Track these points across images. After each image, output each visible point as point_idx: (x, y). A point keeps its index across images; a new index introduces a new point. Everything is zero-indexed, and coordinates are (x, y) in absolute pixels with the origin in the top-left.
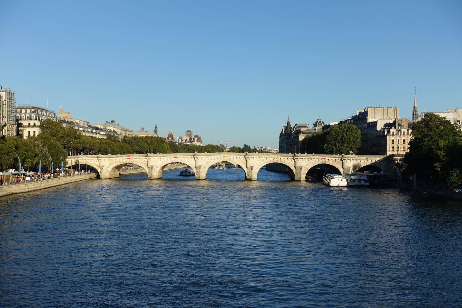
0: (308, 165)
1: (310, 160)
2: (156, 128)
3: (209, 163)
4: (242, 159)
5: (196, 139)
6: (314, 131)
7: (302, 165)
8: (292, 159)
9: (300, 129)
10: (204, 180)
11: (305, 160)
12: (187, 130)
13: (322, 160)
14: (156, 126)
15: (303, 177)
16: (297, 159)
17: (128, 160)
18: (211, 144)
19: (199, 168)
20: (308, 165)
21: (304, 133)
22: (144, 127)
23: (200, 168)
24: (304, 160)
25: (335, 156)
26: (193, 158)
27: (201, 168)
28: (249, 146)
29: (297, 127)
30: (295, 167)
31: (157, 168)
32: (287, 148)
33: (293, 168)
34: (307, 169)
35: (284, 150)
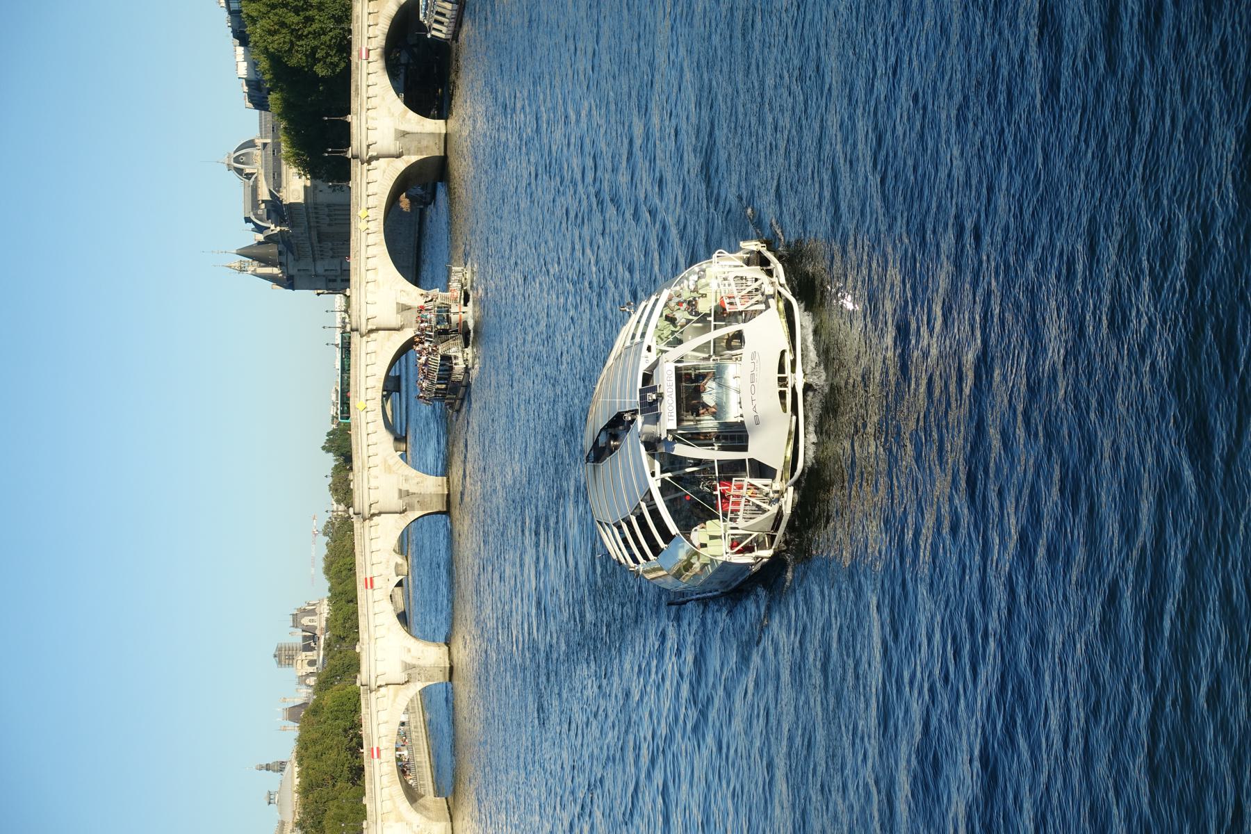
0: (389, 109)
1: (372, 103)
2: (268, 767)
3: (391, 462)
4: (372, 347)
5: (305, 621)
6: (270, 149)
7: (393, 131)
8: (370, 167)
9: (263, 201)
10: (448, 481)
11: (373, 119)
12: (274, 661)
13: (370, 60)
14: (261, 768)
15: (435, 126)
16: (368, 146)
17: (383, 754)
18: (322, 565)
19: (407, 499)
20: (389, 109)
21: (277, 179)
22: (266, 794)
23: (408, 493)
24: (371, 124)
25: (358, 17)
26: (372, 523)
27: (408, 491)
28: (329, 434)
29: (256, 215)
30: (399, 156)
31: (409, 650)
32: (332, 257)
33: (401, 165)
34: (407, 112)
35: (338, 268)
